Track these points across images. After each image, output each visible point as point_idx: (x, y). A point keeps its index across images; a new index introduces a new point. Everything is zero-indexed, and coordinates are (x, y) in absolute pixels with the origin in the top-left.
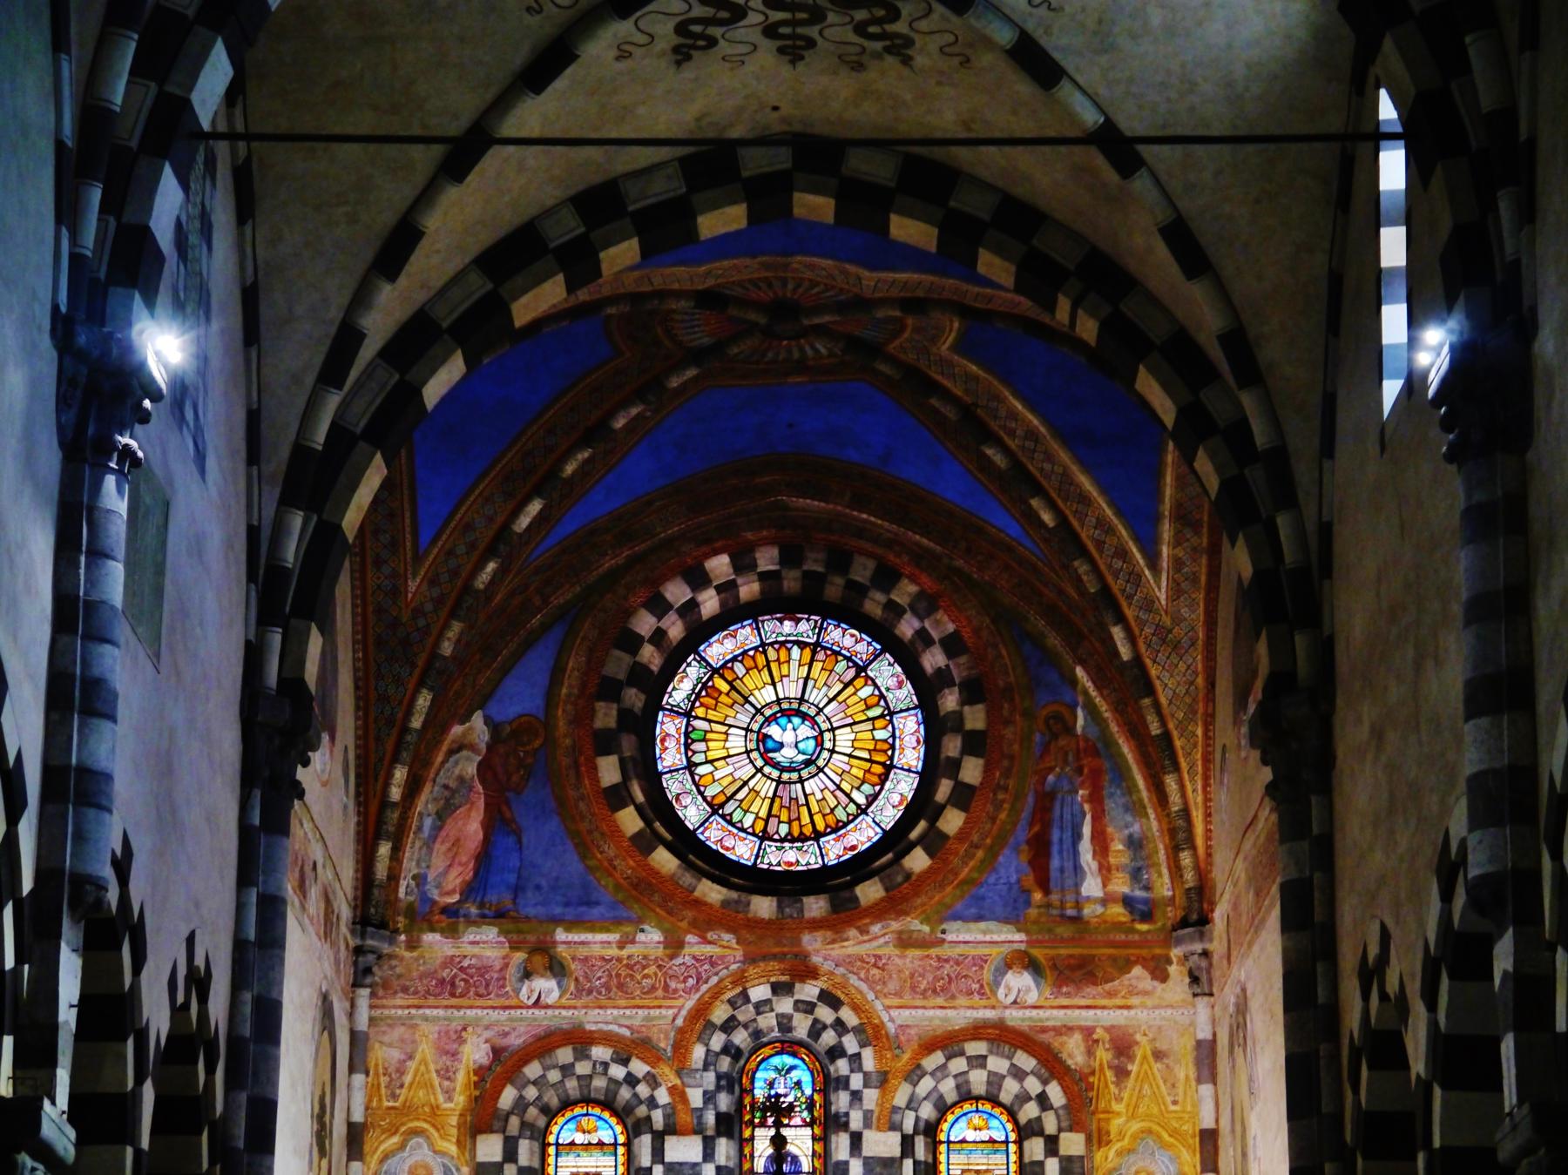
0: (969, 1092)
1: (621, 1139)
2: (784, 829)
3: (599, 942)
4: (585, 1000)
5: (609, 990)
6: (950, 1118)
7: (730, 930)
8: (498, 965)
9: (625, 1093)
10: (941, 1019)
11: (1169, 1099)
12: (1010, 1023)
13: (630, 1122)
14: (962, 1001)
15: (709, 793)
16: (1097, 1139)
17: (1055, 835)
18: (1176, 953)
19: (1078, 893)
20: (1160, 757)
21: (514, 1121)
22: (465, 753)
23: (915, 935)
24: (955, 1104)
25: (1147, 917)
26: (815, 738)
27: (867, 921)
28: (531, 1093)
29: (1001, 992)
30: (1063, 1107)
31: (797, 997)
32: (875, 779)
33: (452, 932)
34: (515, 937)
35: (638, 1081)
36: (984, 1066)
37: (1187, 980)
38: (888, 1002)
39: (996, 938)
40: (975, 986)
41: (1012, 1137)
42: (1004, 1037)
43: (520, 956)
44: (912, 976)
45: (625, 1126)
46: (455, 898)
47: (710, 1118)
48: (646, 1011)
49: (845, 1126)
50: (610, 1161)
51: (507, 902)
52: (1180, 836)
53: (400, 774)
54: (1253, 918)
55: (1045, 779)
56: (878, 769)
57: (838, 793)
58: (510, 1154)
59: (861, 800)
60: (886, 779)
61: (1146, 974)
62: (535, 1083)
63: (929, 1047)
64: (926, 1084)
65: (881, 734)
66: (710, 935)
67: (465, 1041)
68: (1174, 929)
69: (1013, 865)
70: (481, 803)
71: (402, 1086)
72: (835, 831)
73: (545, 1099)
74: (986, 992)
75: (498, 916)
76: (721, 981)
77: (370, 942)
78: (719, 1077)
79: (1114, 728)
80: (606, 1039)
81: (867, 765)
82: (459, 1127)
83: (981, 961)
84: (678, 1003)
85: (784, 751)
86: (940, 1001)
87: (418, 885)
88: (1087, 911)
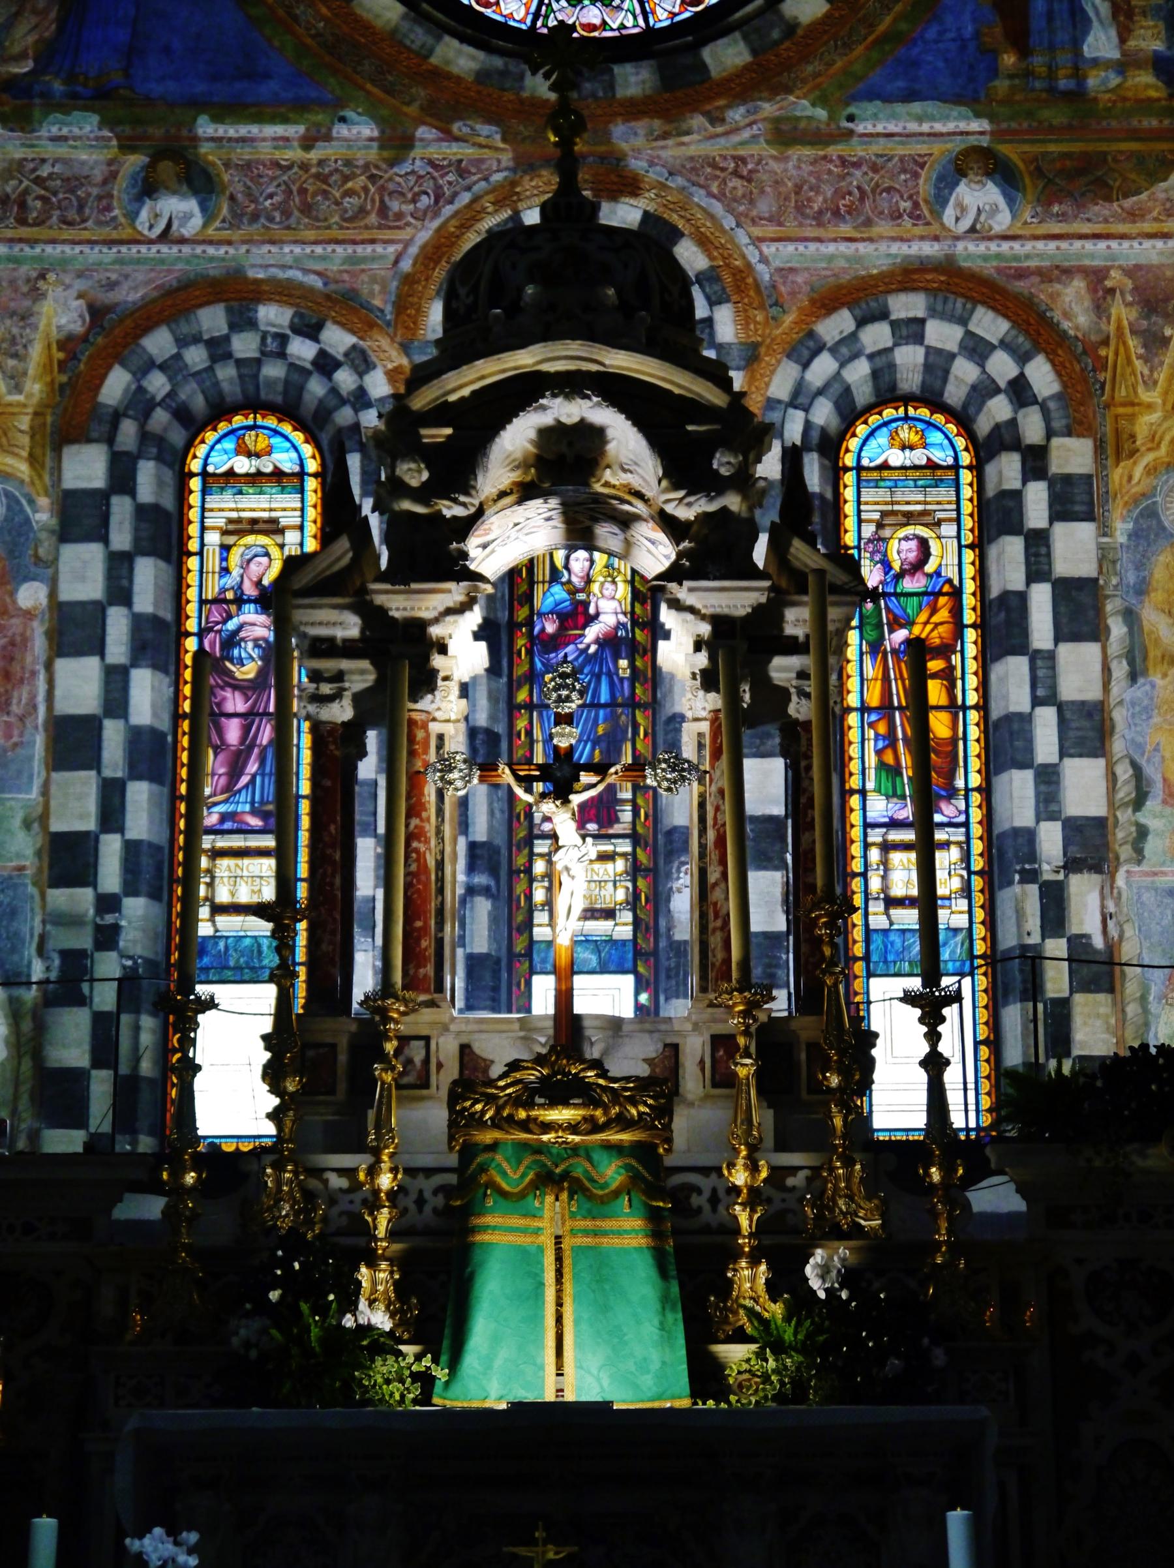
0: (893, 386)
1: (312, 466)
3: (272, 139)
4: (246, 230)
5: (287, 214)
6: (862, 430)
7: (489, 121)
8: (98, 174)
9: (316, 387)
10: (848, 259)
13: (325, 437)
14: (883, 228)
16: (1115, 447)
19: (1077, 53)
21: (128, 430)
23: (802, 125)
27: (721, 102)
28: (158, 384)
29: (949, 214)
30: (1058, 397)
34: (127, 130)
35: (337, 365)
38: (757, 231)
39: (939, 127)
40: (905, 205)
41: (966, 459)
42: (954, 286)
43: (135, 161)
44: (798, 189)
45: (318, 446)
46: (26, 67)
48: (350, 249)
50: (293, 500)
51: (117, 77)
62: (163, 367)
63: (828, 301)
64: (823, 367)
66: (457, 127)
67: (44, 295)
76: (475, 199)
80: (282, 292)
84: (404, 235)
86: (846, 229)
88: (1092, 82)
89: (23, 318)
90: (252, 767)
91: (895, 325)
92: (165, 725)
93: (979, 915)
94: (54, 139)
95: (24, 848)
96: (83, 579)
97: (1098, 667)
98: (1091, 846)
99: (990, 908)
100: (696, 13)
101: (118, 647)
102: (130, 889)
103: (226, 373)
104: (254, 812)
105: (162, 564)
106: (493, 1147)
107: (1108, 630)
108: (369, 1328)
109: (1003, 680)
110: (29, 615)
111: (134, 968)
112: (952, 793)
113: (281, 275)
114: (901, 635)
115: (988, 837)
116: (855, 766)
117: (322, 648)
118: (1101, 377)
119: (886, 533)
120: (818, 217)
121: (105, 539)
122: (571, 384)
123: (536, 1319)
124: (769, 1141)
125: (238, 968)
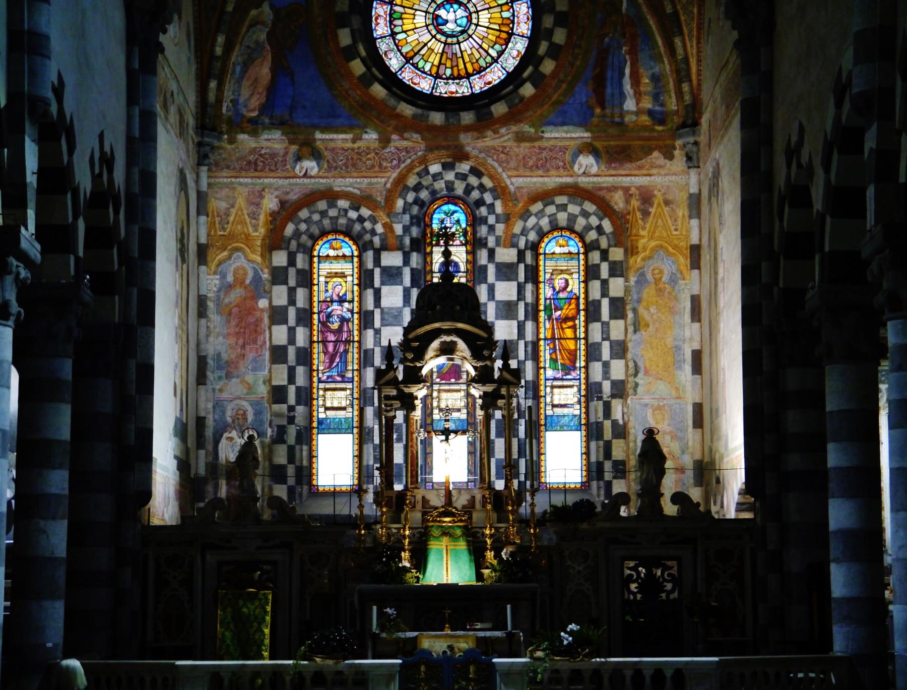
0: (557, 225)
1: (356, 253)
2: (448, 72)
3: (341, 139)
4: (333, 173)
5: (347, 167)
6: (546, 240)
7: (417, 132)
8: (282, 152)
9: (357, 227)
10: (541, 183)
11: (673, 228)
12: (581, 185)
13: (360, 243)
14: (553, 172)
15: (404, 50)
16: (631, 251)
17: (609, 74)
18: (679, 143)
19: (622, 109)
20: (671, 27)
21: (294, 244)
22: (259, 26)
24: (548, 232)
25: (662, 122)
26: (467, 17)
27: (497, 126)
28: (303, 227)
29: (576, 167)
30: (611, 233)
31: (457, 171)
32: (502, 42)
33: (254, 133)
34: (292, 136)
35: (365, 220)
36: (565, 210)
37: (685, 159)
38: (510, 173)
39: (573, 135)
40: (561, 164)
41: (582, 250)
42: (577, 193)
43: (294, 148)
44: (524, 158)
45: (358, 246)
47: (407, 241)
49: (485, 245)
50: (349, 266)
51: (287, 117)
52: (682, 74)
53: (221, 39)
54: (725, 121)
55: (604, 39)
56: (504, 35)
57: (481, 50)
58: (292, 262)
59: (494, 54)
60: (509, 42)
61: (661, 156)
62: (305, 221)
63: (534, 199)
64: (532, 221)
65: (506, 14)
66: (405, 135)
68: (678, 129)
69: (583, 93)
70: (269, 57)
71: (228, 223)
72: (479, 73)
73: (311, 230)
74: (568, 167)
75: (280, 124)
76: (412, 162)
77: (206, 139)
78: (412, 217)
79: (645, 9)
80: (346, 195)
81: (498, 33)
82: (262, 246)
83: (564, 149)
85: (448, 25)
86: (540, 172)
87: (233, 106)
88: (627, 119)
89: (257, 205)
90: (337, 360)
91: (557, 206)
92: (307, 346)
93: (583, 410)
95: (263, 390)
96: (280, 298)
97: (623, 328)
98: (620, 390)
99: (587, 408)
100: (490, 88)
101: (292, 321)
102: (298, 402)
104: (338, 375)
105: (306, 290)
106: (432, 526)
107: (627, 315)
108: (405, 567)
109: (593, 330)
110: (262, 310)
111: (300, 430)
112: (575, 368)
114: (559, 313)
115: (587, 384)
116: (542, 359)
117: (388, 398)
119: (554, 277)
120: (531, 168)
121: (287, 284)
122: (448, 332)
123: (442, 565)
124: (496, 521)
125: (334, 429)
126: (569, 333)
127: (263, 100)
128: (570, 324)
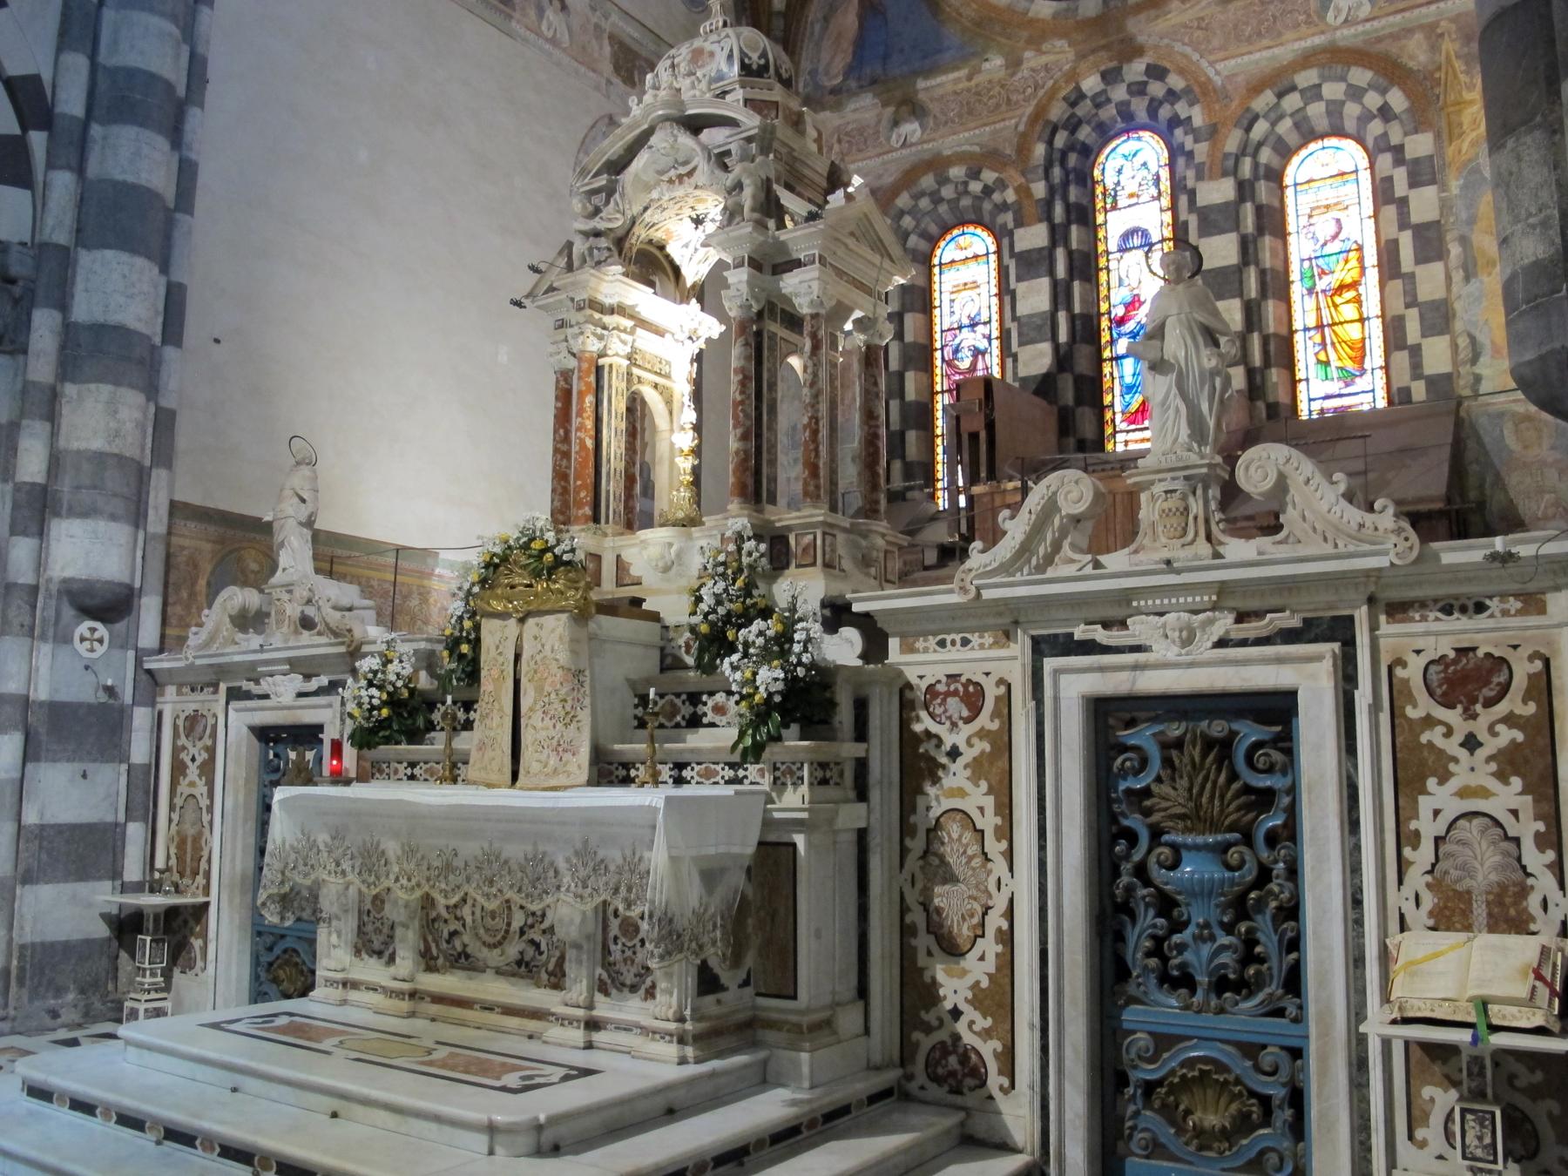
1: (993, 248)
5: (960, 116)
12: (1341, 44)
14: (1289, 35)
36: (1319, 97)
38: (1212, 58)
43: (891, 109)
44: (1236, 27)
62: (909, 213)
63: (1256, 89)
84: (1018, 112)
86: (1265, 42)
94: (855, 110)
97: (1442, 276)
103: (943, 209)
107: (1448, 251)
112: (1363, 371)
113: (958, 149)
114: (1326, 279)
118: (1437, 91)
120: (1249, 40)
126: (1349, 312)
127: (849, 59)
128: (1350, 294)
